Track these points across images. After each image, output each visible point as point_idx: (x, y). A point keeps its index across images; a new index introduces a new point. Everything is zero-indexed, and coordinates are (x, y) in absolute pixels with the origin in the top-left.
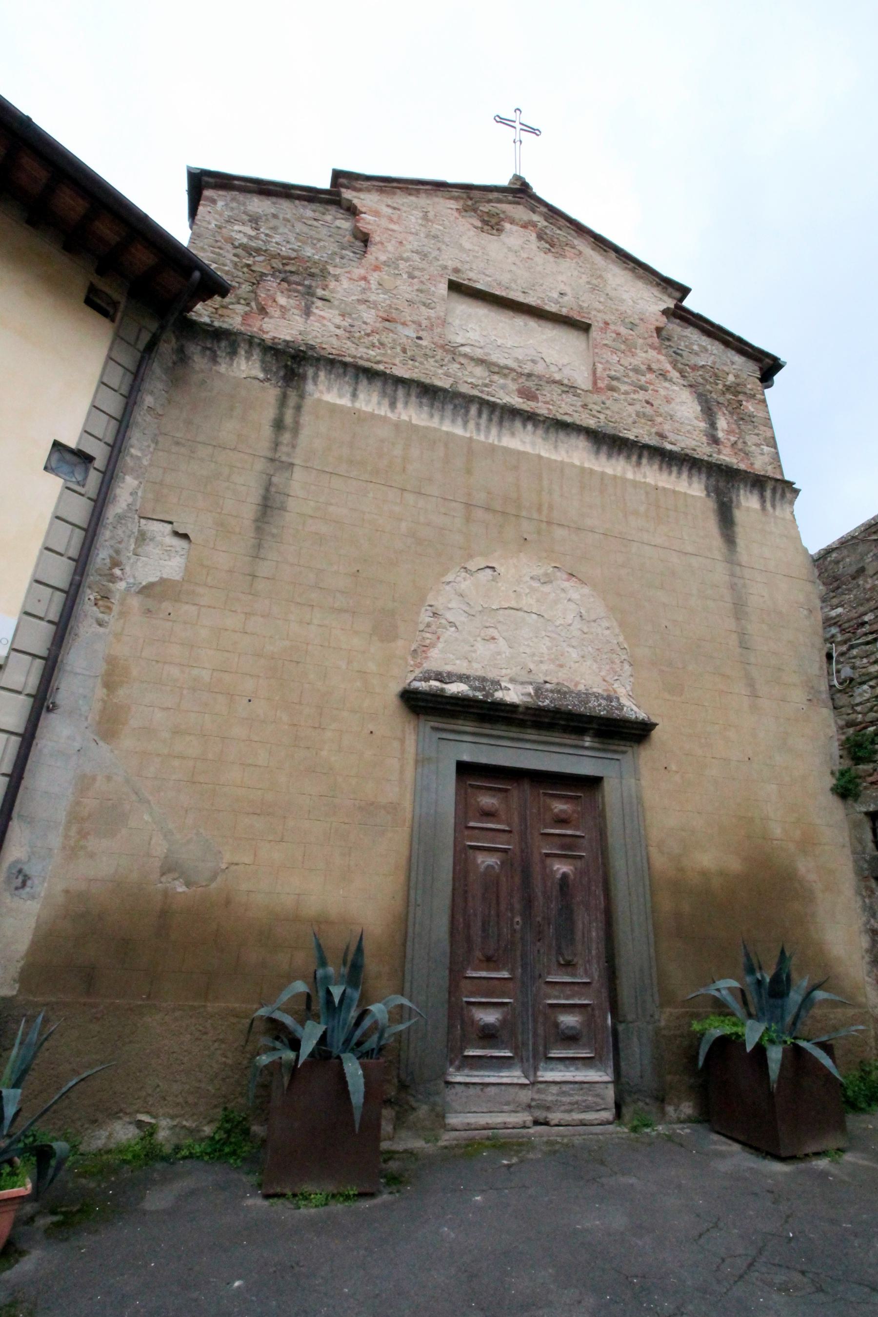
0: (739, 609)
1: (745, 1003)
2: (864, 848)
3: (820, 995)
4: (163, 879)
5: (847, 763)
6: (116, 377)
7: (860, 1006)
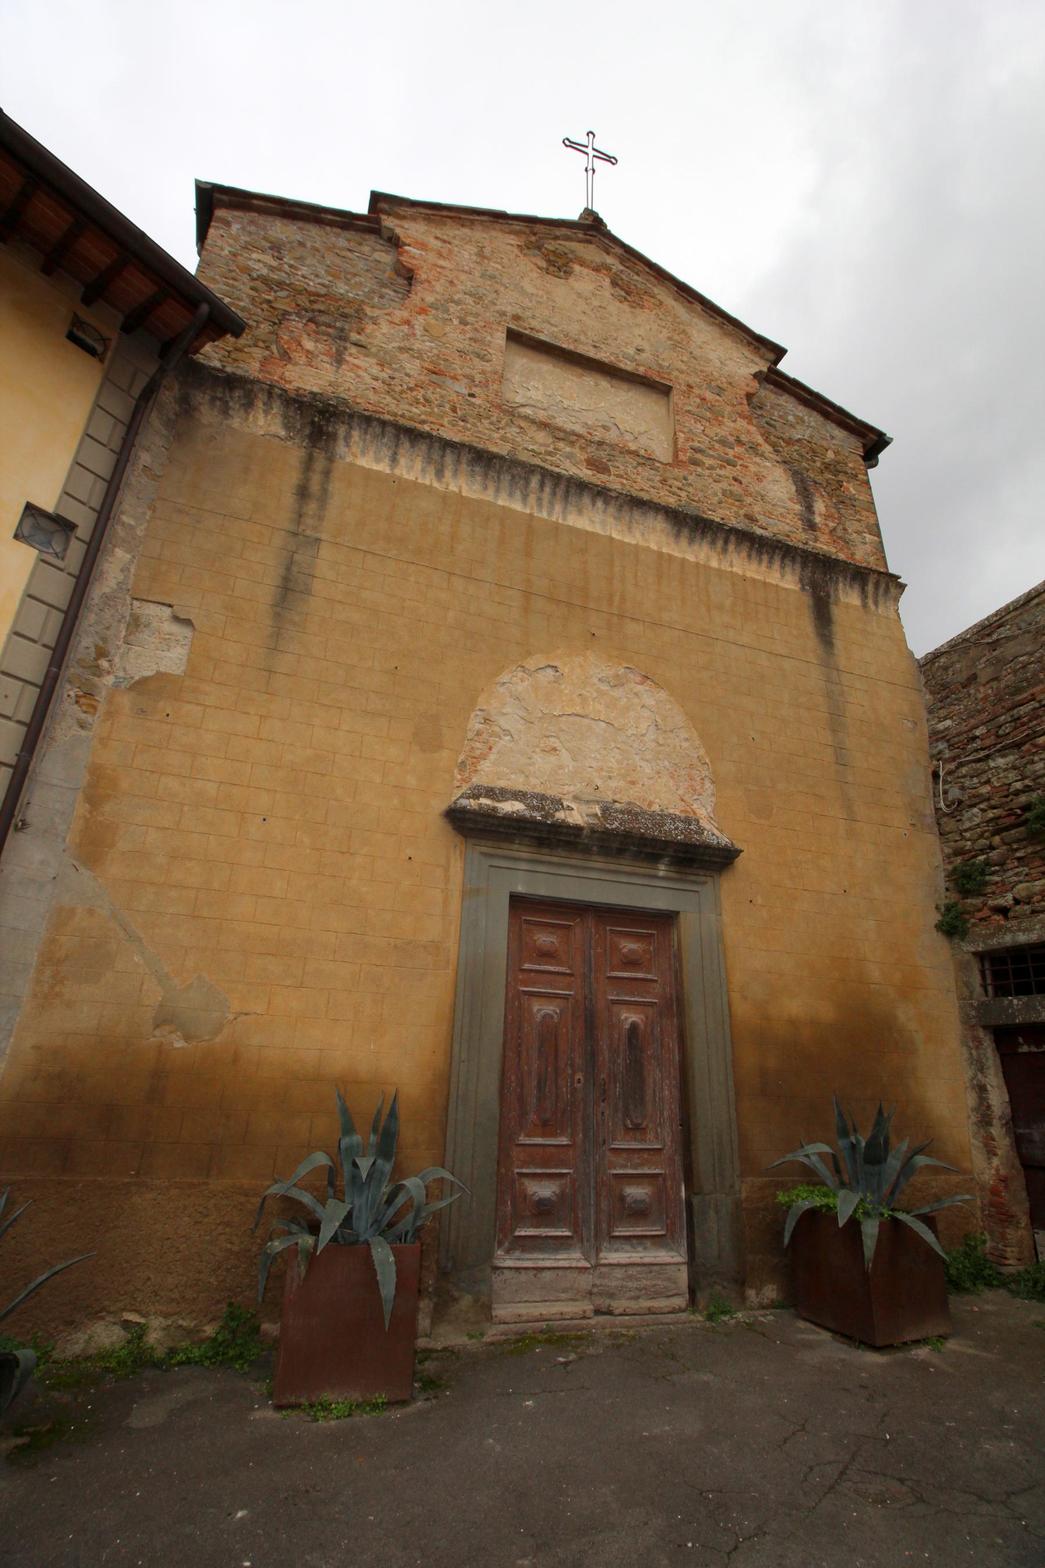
0: (836, 719)
1: (838, 1171)
2: (971, 992)
3: (921, 1160)
4: (157, 1032)
5: (954, 897)
6: (107, 430)
7: (965, 1172)
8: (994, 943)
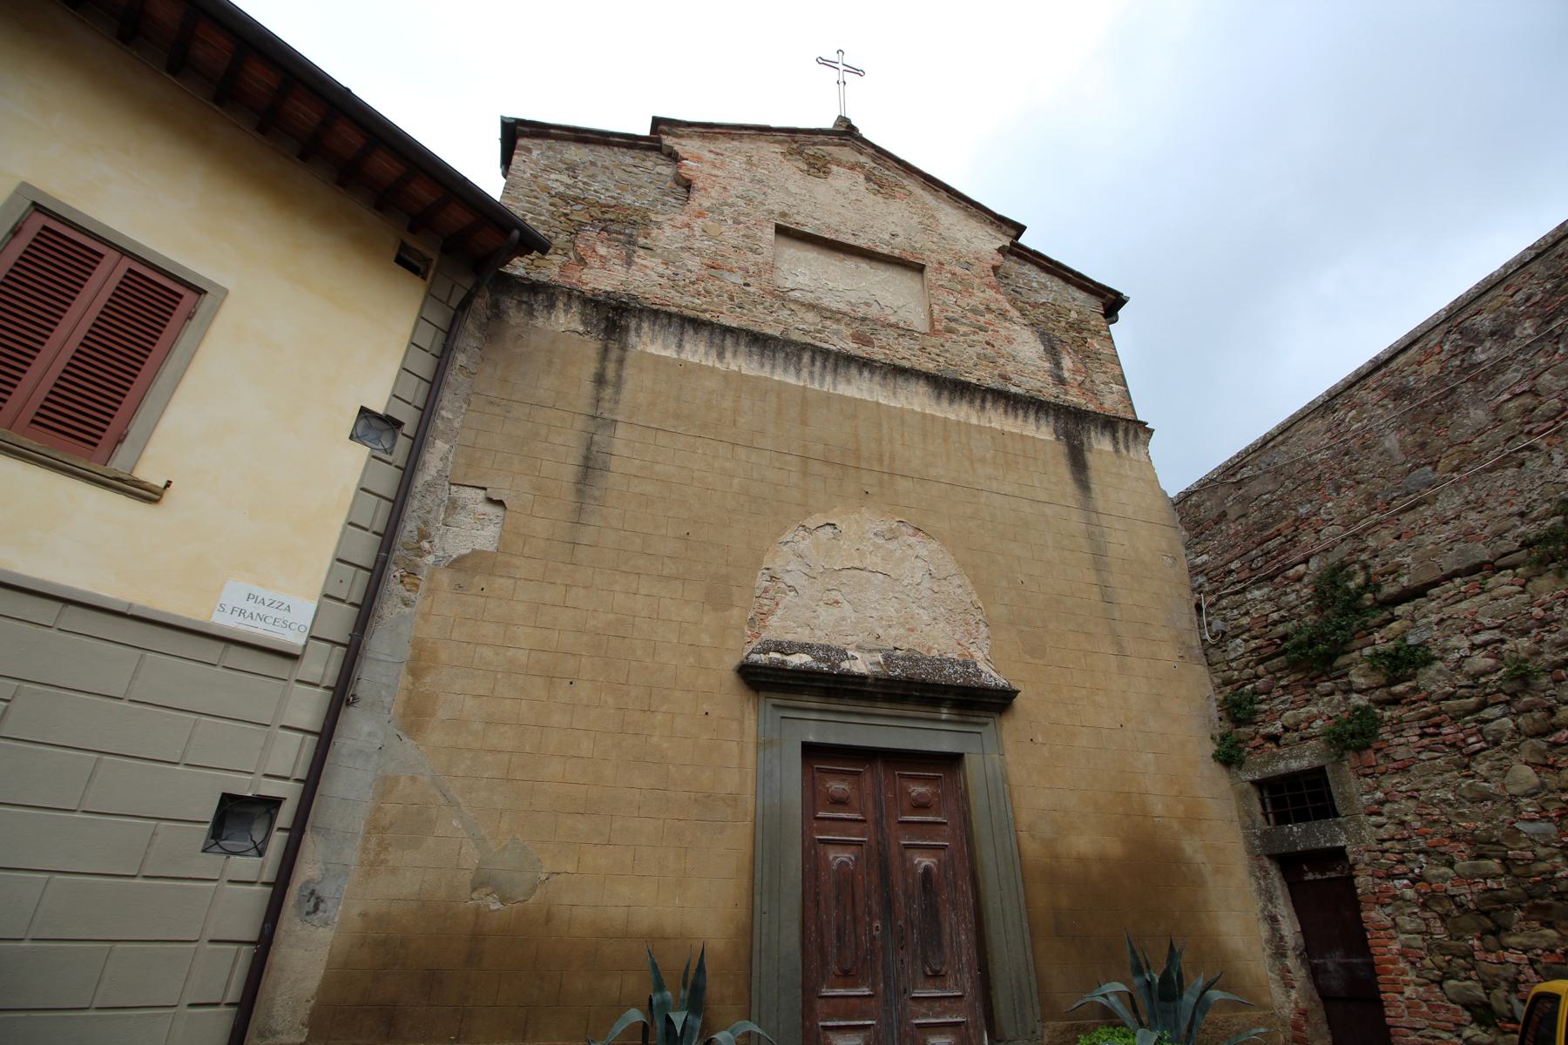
0: (1099, 559)
1: (1135, 1010)
2: (1254, 822)
3: (1215, 995)
4: (474, 895)
5: (1227, 726)
6: (428, 337)
7: (1264, 1007)
8: (1269, 770)
